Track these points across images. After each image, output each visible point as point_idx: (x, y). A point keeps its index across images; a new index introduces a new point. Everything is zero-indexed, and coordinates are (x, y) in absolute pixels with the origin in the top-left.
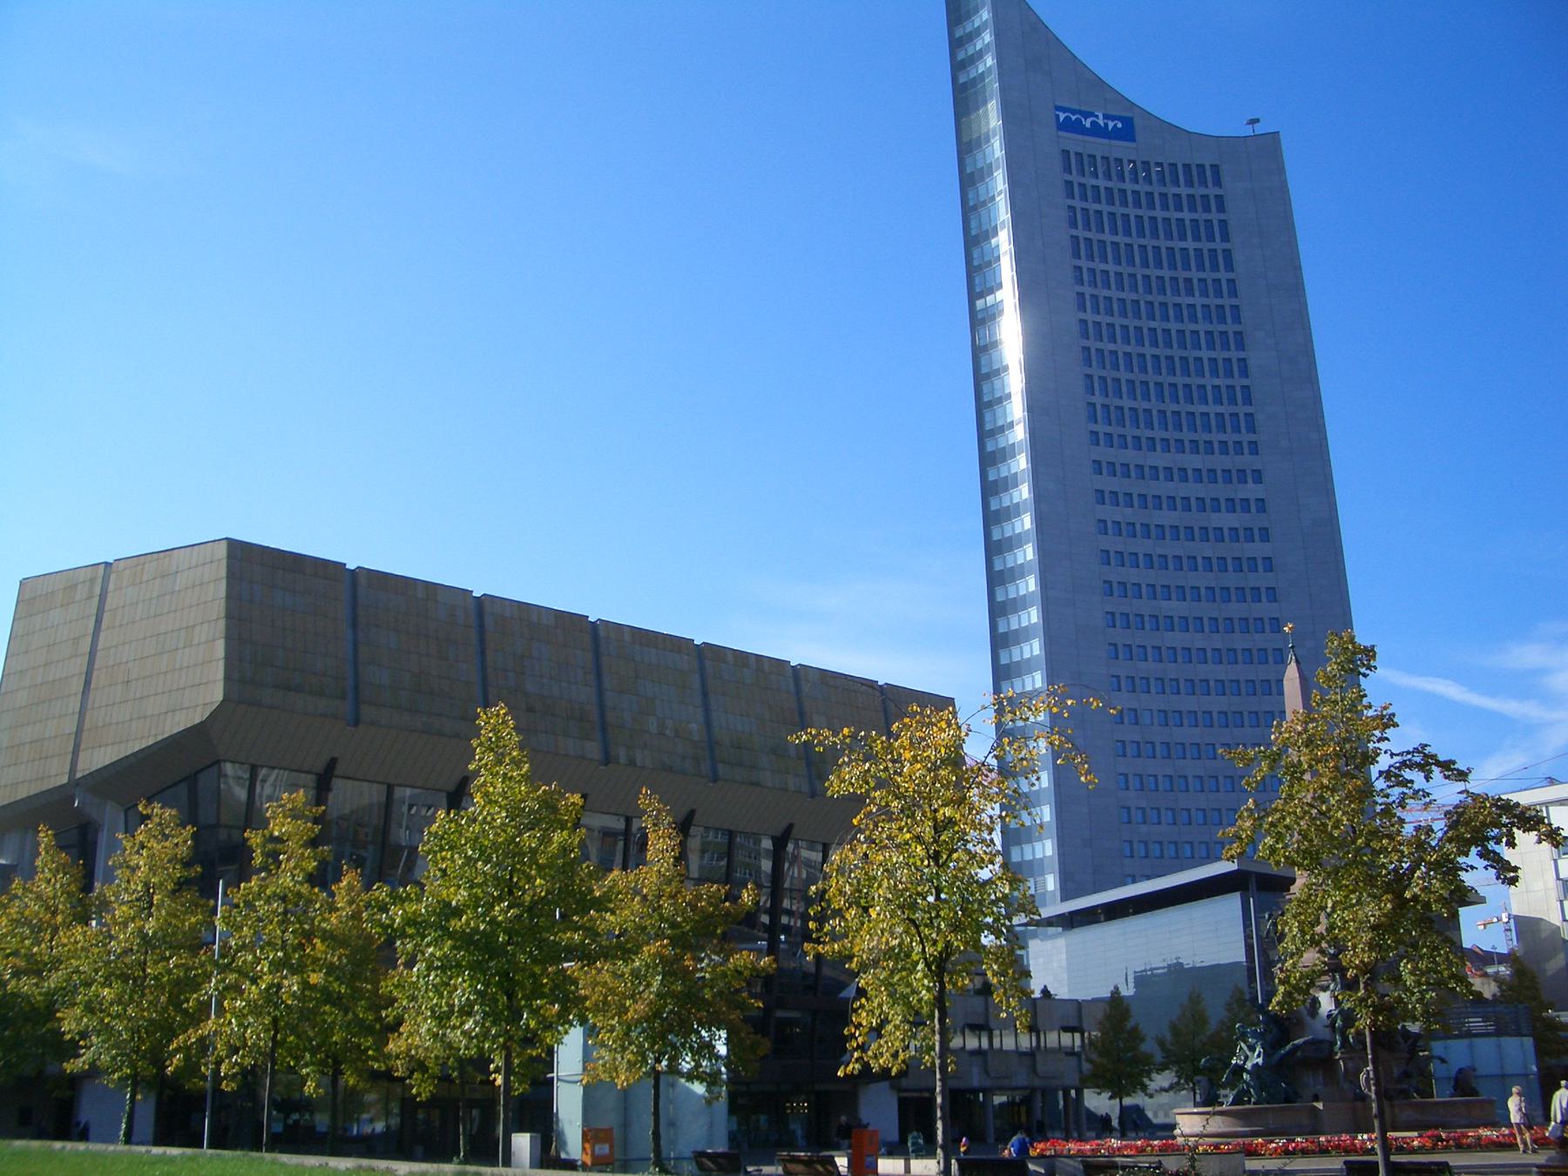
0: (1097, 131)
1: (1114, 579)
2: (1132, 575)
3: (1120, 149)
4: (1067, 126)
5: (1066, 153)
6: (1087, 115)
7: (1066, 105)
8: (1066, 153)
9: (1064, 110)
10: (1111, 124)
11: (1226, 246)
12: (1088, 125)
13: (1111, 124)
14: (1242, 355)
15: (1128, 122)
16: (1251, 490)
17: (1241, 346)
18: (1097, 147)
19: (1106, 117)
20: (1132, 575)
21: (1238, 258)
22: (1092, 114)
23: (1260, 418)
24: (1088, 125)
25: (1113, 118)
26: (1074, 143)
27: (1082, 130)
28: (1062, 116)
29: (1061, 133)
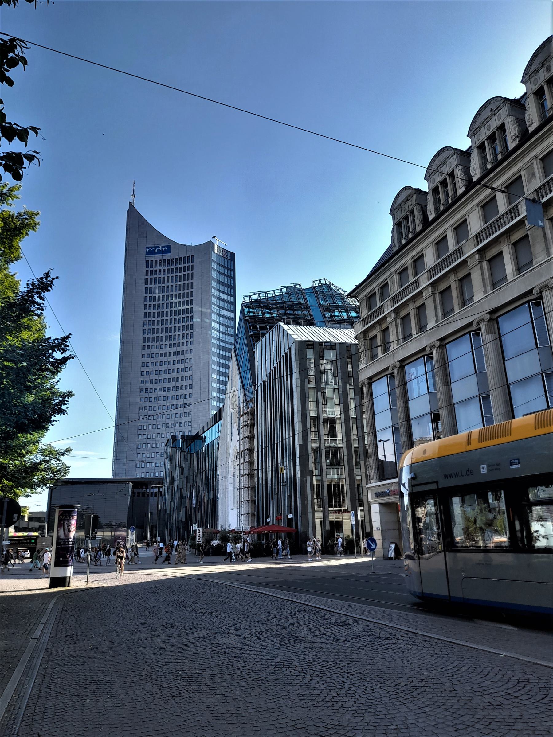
0: (160, 252)
3: (166, 257)
5: (147, 261)
6: (156, 248)
8: (147, 261)
10: (164, 249)
12: (156, 251)
13: (164, 249)
15: (169, 247)
16: (188, 356)
18: (158, 257)
19: (163, 247)
21: (195, 284)
23: (194, 333)
24: (156, 251)
26: (151, 258)
28: (148, 250)
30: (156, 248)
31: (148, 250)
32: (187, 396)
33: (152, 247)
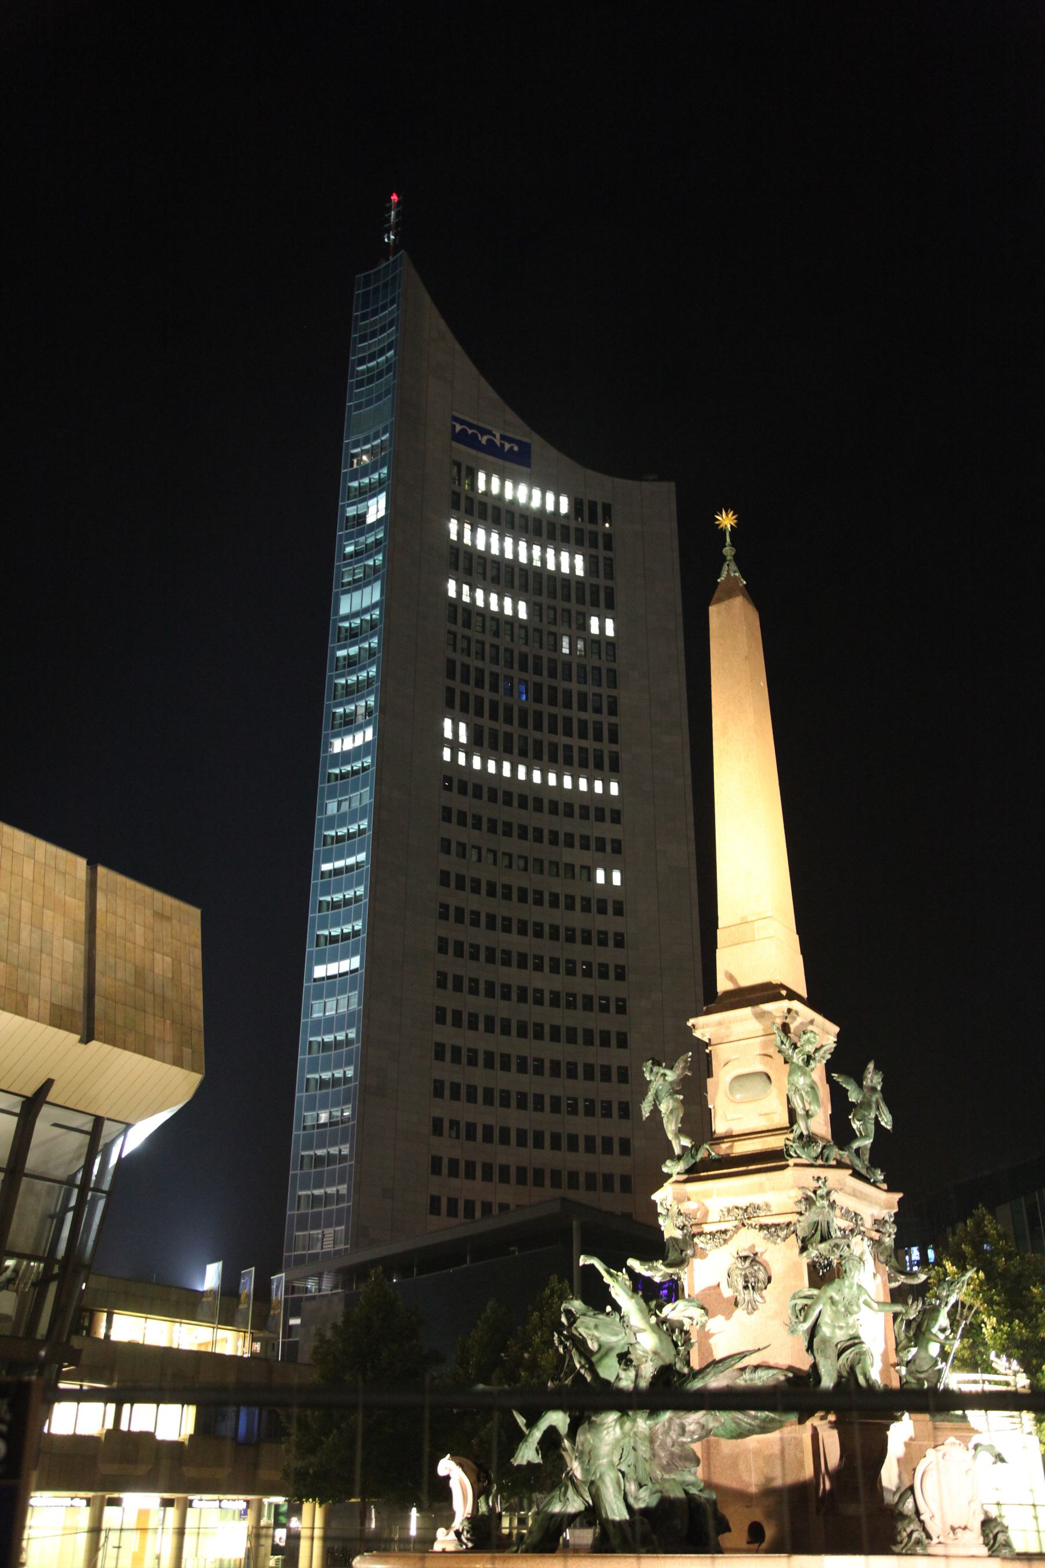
1: (453, 903)
2: (472, 902)
4: (461, 438)
6: (484, 432)
7: (467, 419)
9: (462, 422)
10: (507, 446)
11: (609, 583)
12: (484, 442)
14: (614, 692)
17: (613, 683)
19: (503, 438)
20: (472, 902)
22: (490, 433)
24: (484, 442)
25: (510, 440)
27: (479, 447)
28: (458, 428)
29: (455, 444)
30: (484, 432)
31: (458, 428)
32: (581, 968)
33: (471, 426)
